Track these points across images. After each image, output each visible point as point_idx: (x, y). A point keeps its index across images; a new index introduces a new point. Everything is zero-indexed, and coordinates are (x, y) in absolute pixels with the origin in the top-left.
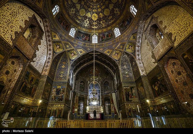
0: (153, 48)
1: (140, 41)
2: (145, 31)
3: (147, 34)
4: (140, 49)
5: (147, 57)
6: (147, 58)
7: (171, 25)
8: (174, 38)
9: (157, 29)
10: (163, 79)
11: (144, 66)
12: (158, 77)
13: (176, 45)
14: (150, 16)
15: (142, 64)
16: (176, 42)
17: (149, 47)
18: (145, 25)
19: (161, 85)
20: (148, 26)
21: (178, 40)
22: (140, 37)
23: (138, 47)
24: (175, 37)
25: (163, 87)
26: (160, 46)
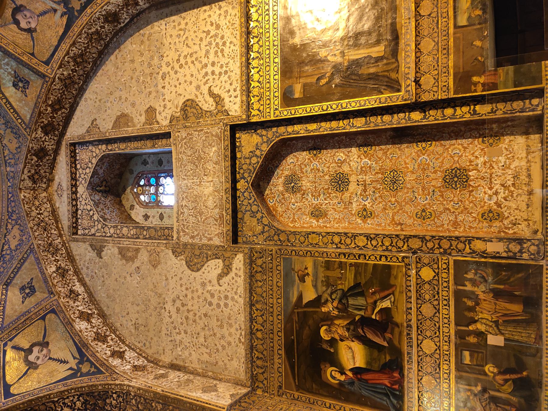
0: (168, 237)
1: (78, 288)
2: (74, 228)
3: (93, 231)
4: (105, 323)
5: (168, 306)
6: (173, 310)
7: (164, 87)
8: (211, 100)
9: (121, 201)
10: (328, 265)
11: (192, 373)
12: (300, 297)
13: (237, 107)
14: (56, 152)
15: (173, 375)
16: (227, 100)
17: (143, 256)
18: (54, 212)
19: (351, 301)
20: (74, 199)
21: (228, 87)
22: (62, 272)
23: (89, 321)
24: (211, 94)
25: (362, 294)
26: (189, 183)
